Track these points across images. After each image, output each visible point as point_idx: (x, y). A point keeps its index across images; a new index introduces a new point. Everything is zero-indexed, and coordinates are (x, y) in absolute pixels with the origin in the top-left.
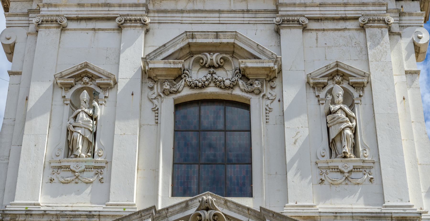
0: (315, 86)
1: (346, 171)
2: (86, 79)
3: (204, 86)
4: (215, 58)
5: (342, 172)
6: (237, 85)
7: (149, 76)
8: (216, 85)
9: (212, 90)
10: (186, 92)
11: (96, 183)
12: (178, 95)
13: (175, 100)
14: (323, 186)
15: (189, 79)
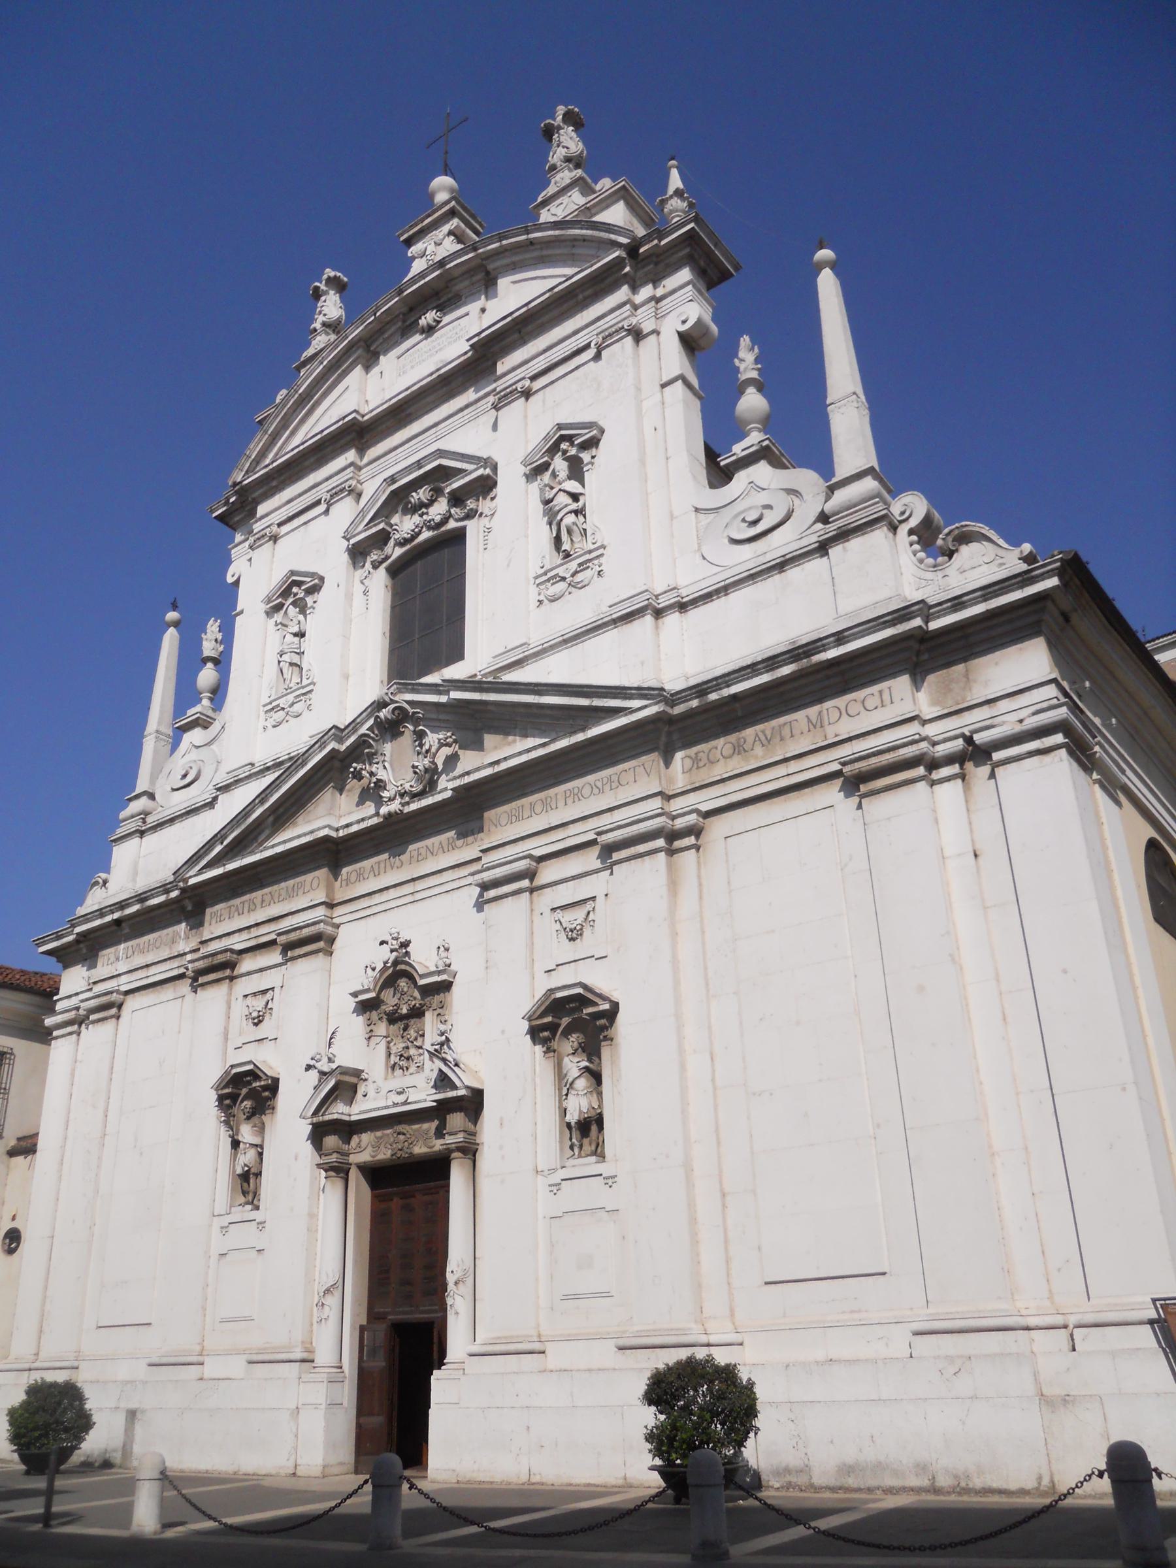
0: (538, 470)
1: (568, 575)
2: (295, 590)
3: (413, 538)
4: (422, 494)
5: (564, 579)
6: (451, 516)
7: (357, 554)
8: (429, 528)
9: (426, 535)
10: (399, 551)
11: (306, 713)
12: (390, 561)
13: (388, 569)
14: (543, 607)
15: (397, 536)
